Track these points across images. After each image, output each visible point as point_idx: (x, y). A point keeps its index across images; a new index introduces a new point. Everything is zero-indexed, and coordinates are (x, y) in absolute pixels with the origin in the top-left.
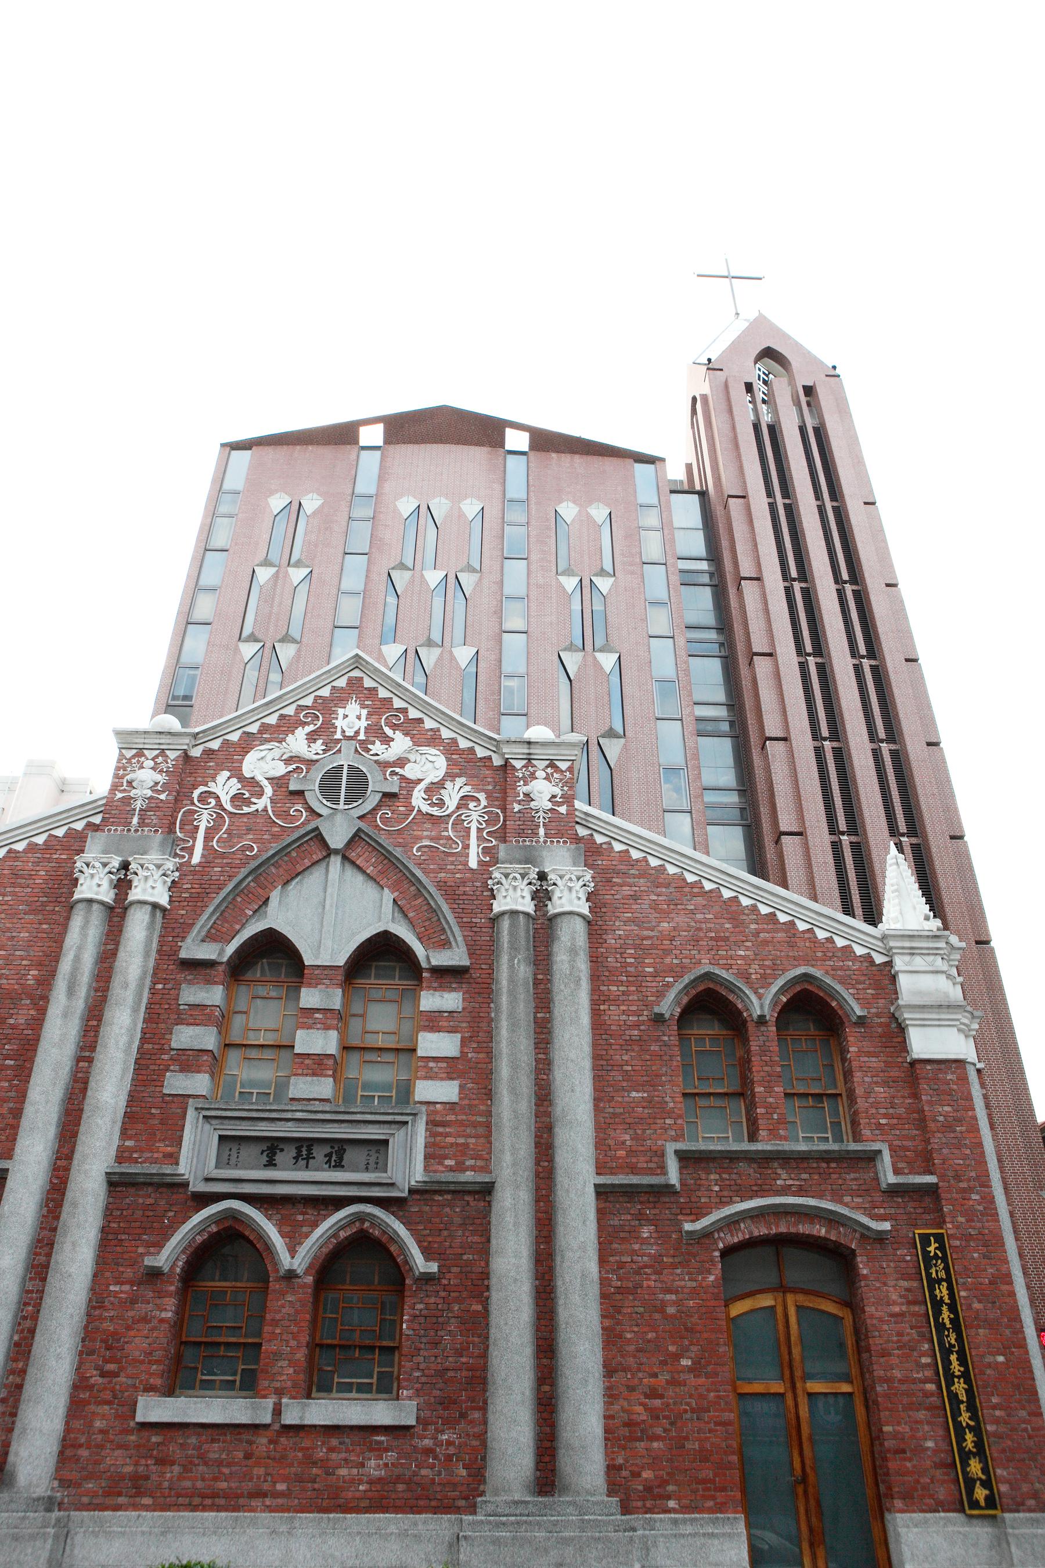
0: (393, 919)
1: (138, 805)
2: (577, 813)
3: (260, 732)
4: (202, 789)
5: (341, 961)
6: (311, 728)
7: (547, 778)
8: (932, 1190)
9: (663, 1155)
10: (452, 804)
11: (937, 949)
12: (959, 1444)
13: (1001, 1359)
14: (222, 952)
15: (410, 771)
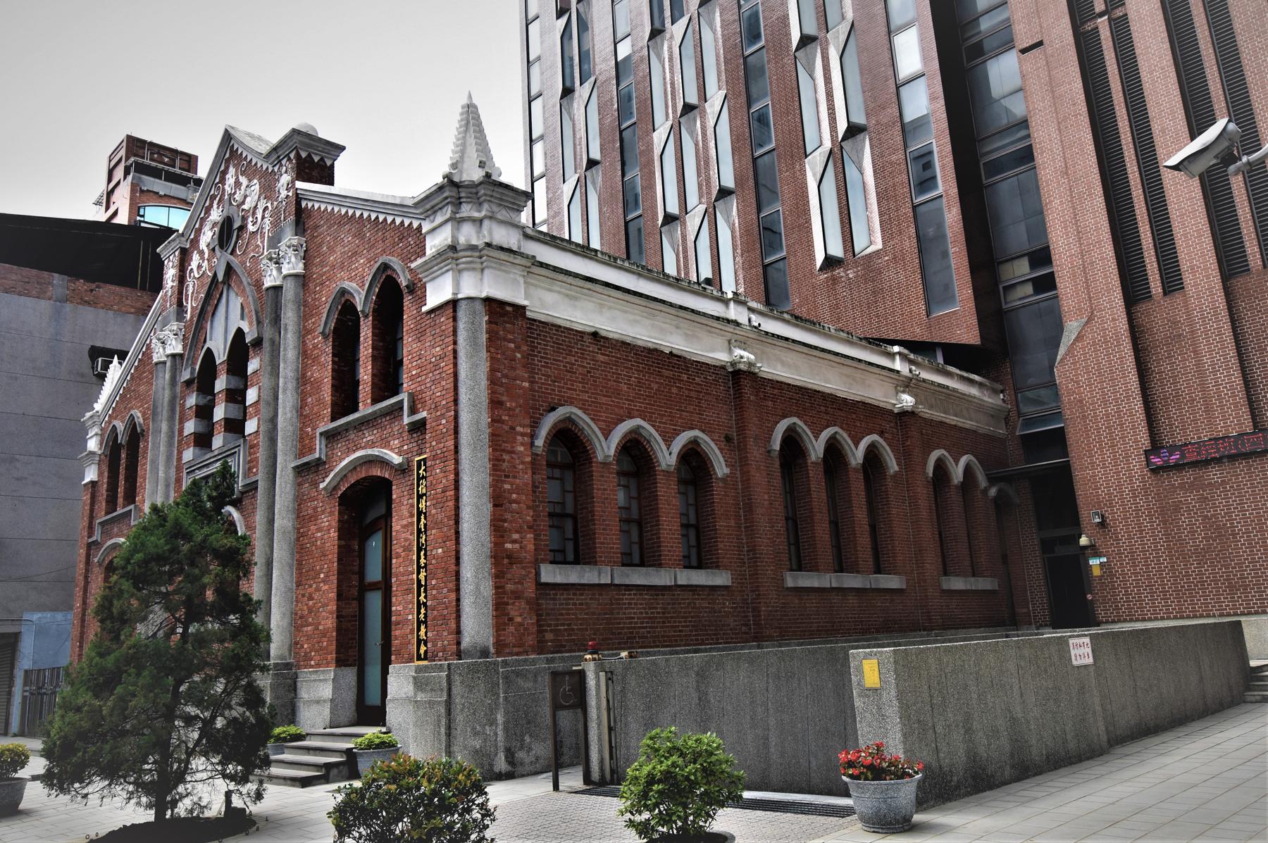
0: (242, 318)
1: (169, 294)
2: (299, 192)
3: (205, 214)
4: (190, 268)
5: (225, 358)
6: (217, 199)
7: (286, 172)
8: (423, 422)
9: (313, 438)
10: (259, 219)
11: (446, 198)
12: (418, 616)
13: (440, 551)
14: (193, 369)
15: (245, 207)
